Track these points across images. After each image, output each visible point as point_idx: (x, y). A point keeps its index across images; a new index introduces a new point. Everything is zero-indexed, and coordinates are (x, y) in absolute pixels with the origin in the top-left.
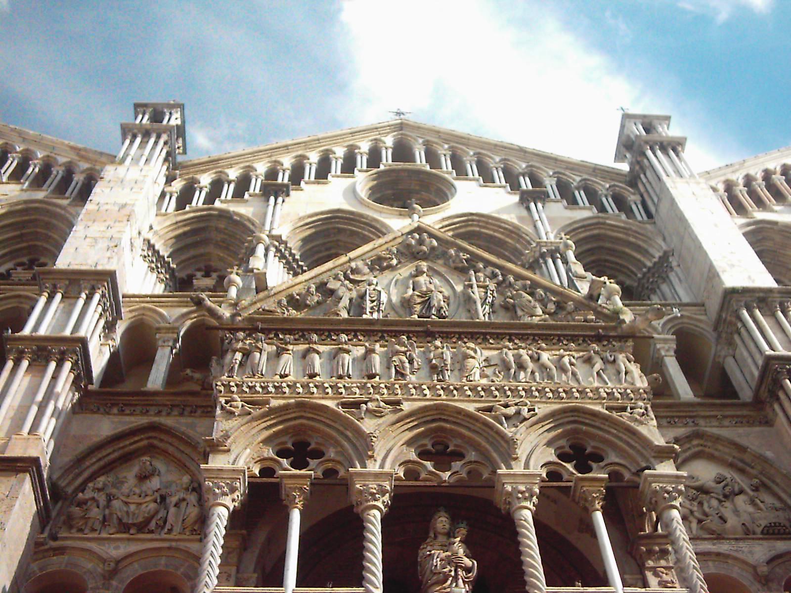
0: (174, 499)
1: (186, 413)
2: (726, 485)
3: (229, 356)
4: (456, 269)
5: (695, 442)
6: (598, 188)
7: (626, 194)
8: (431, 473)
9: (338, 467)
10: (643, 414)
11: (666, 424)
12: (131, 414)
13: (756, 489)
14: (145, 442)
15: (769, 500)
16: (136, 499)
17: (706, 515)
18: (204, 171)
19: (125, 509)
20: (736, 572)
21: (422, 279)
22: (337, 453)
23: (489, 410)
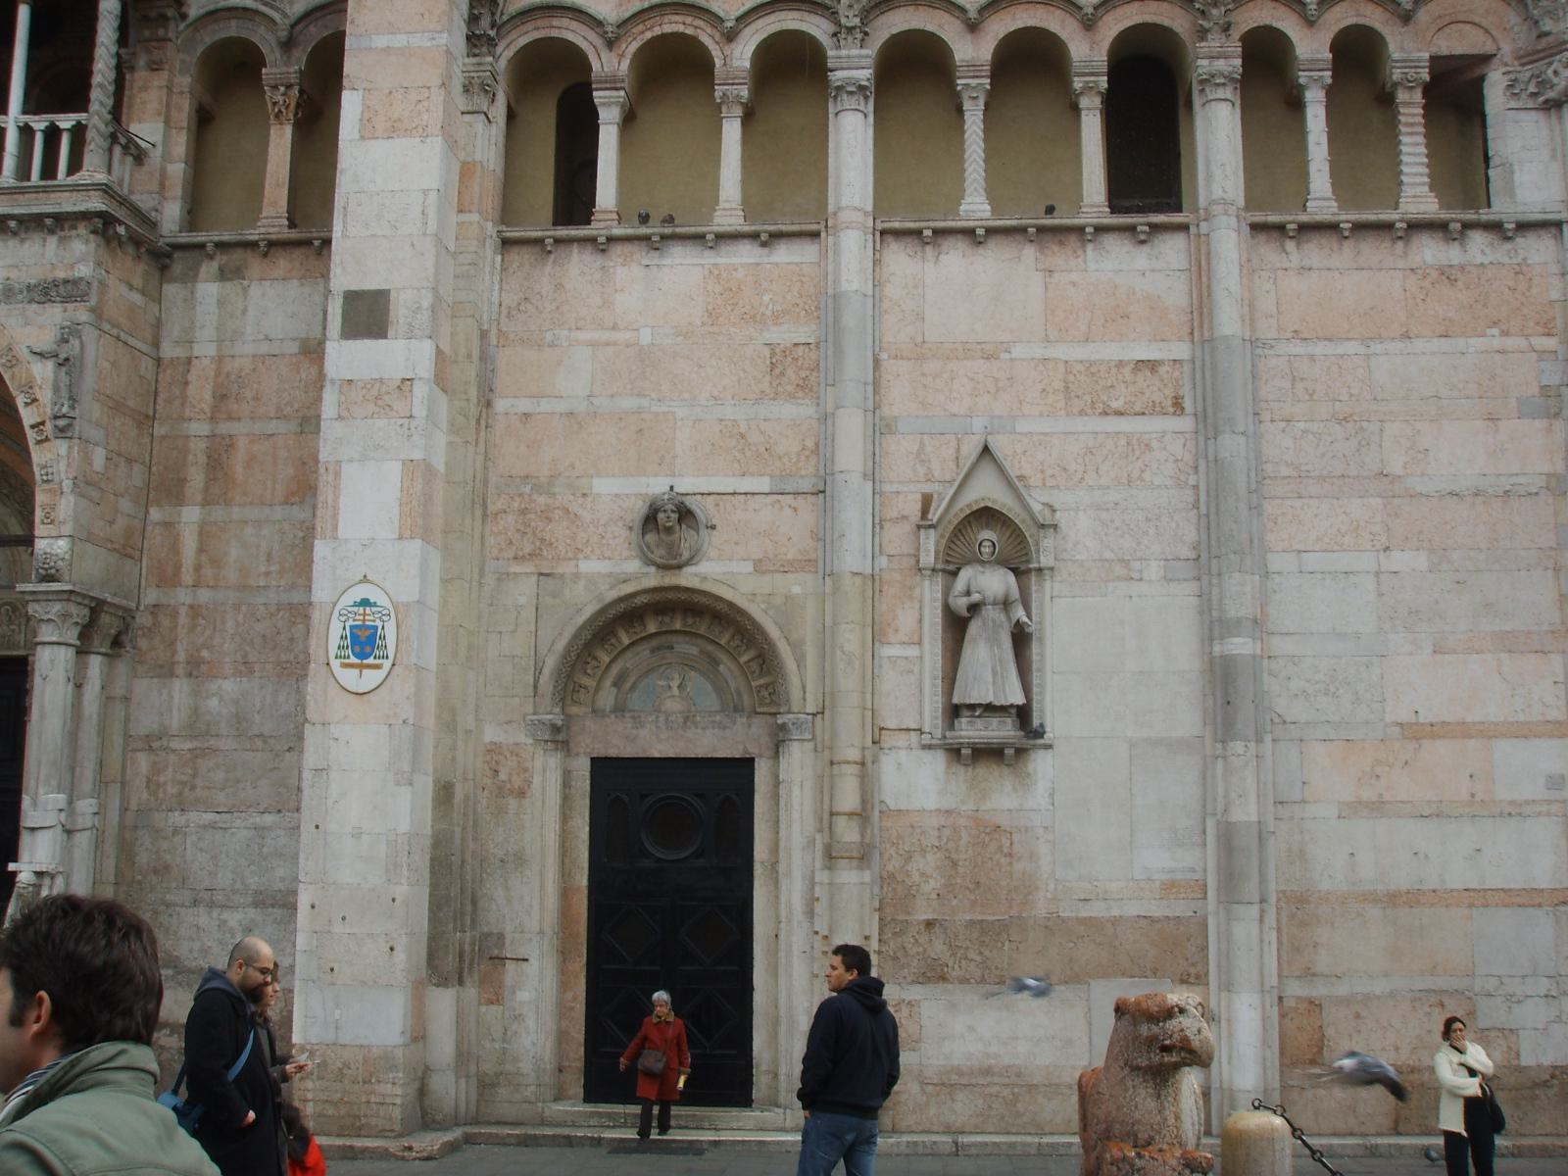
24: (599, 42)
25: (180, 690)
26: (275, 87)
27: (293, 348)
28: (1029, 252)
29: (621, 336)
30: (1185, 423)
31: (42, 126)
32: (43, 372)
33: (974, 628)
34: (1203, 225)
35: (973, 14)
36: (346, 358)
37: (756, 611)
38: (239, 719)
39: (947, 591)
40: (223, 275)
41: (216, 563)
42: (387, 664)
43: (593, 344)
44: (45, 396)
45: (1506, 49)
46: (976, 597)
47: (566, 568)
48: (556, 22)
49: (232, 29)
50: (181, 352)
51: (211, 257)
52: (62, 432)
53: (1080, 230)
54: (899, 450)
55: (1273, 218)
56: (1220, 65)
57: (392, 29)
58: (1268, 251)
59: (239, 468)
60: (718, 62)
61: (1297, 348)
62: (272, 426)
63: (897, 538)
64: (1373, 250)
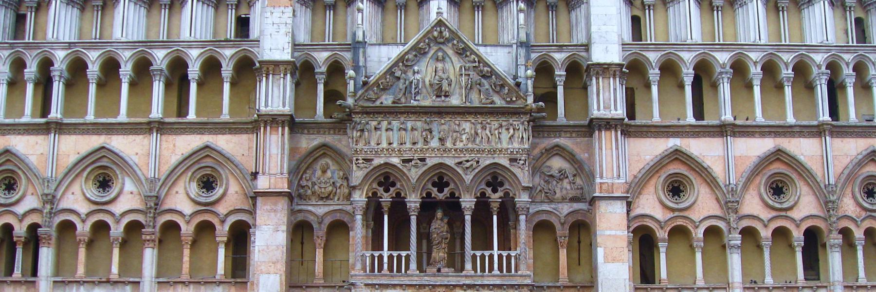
0: (338, 185)
1: (336, 132)
2: (562, 174)
3: (355, 132)
4: (457, 53)
5: (555, 149)
8: (436, 195)
9: (401, 192)
10: (523, 164)
11: (546, 135)
12: (313, 134)
13: (574, 176)
14: (322, 152)
16: (323, 185)
17: (549, 190)
19: (320, 191)
20: (553, 220)
21: (440, 65)
22: (401, 185)
23: (460, 163)
24: (658, 227)
26: (561, 237)
31: (506, 254)
35: (766, 223)
48: (645, 220)
49: (544, 217)
51: (545, 290)
53: (798, 287)
57: (611, 229)
60: (694, 235)
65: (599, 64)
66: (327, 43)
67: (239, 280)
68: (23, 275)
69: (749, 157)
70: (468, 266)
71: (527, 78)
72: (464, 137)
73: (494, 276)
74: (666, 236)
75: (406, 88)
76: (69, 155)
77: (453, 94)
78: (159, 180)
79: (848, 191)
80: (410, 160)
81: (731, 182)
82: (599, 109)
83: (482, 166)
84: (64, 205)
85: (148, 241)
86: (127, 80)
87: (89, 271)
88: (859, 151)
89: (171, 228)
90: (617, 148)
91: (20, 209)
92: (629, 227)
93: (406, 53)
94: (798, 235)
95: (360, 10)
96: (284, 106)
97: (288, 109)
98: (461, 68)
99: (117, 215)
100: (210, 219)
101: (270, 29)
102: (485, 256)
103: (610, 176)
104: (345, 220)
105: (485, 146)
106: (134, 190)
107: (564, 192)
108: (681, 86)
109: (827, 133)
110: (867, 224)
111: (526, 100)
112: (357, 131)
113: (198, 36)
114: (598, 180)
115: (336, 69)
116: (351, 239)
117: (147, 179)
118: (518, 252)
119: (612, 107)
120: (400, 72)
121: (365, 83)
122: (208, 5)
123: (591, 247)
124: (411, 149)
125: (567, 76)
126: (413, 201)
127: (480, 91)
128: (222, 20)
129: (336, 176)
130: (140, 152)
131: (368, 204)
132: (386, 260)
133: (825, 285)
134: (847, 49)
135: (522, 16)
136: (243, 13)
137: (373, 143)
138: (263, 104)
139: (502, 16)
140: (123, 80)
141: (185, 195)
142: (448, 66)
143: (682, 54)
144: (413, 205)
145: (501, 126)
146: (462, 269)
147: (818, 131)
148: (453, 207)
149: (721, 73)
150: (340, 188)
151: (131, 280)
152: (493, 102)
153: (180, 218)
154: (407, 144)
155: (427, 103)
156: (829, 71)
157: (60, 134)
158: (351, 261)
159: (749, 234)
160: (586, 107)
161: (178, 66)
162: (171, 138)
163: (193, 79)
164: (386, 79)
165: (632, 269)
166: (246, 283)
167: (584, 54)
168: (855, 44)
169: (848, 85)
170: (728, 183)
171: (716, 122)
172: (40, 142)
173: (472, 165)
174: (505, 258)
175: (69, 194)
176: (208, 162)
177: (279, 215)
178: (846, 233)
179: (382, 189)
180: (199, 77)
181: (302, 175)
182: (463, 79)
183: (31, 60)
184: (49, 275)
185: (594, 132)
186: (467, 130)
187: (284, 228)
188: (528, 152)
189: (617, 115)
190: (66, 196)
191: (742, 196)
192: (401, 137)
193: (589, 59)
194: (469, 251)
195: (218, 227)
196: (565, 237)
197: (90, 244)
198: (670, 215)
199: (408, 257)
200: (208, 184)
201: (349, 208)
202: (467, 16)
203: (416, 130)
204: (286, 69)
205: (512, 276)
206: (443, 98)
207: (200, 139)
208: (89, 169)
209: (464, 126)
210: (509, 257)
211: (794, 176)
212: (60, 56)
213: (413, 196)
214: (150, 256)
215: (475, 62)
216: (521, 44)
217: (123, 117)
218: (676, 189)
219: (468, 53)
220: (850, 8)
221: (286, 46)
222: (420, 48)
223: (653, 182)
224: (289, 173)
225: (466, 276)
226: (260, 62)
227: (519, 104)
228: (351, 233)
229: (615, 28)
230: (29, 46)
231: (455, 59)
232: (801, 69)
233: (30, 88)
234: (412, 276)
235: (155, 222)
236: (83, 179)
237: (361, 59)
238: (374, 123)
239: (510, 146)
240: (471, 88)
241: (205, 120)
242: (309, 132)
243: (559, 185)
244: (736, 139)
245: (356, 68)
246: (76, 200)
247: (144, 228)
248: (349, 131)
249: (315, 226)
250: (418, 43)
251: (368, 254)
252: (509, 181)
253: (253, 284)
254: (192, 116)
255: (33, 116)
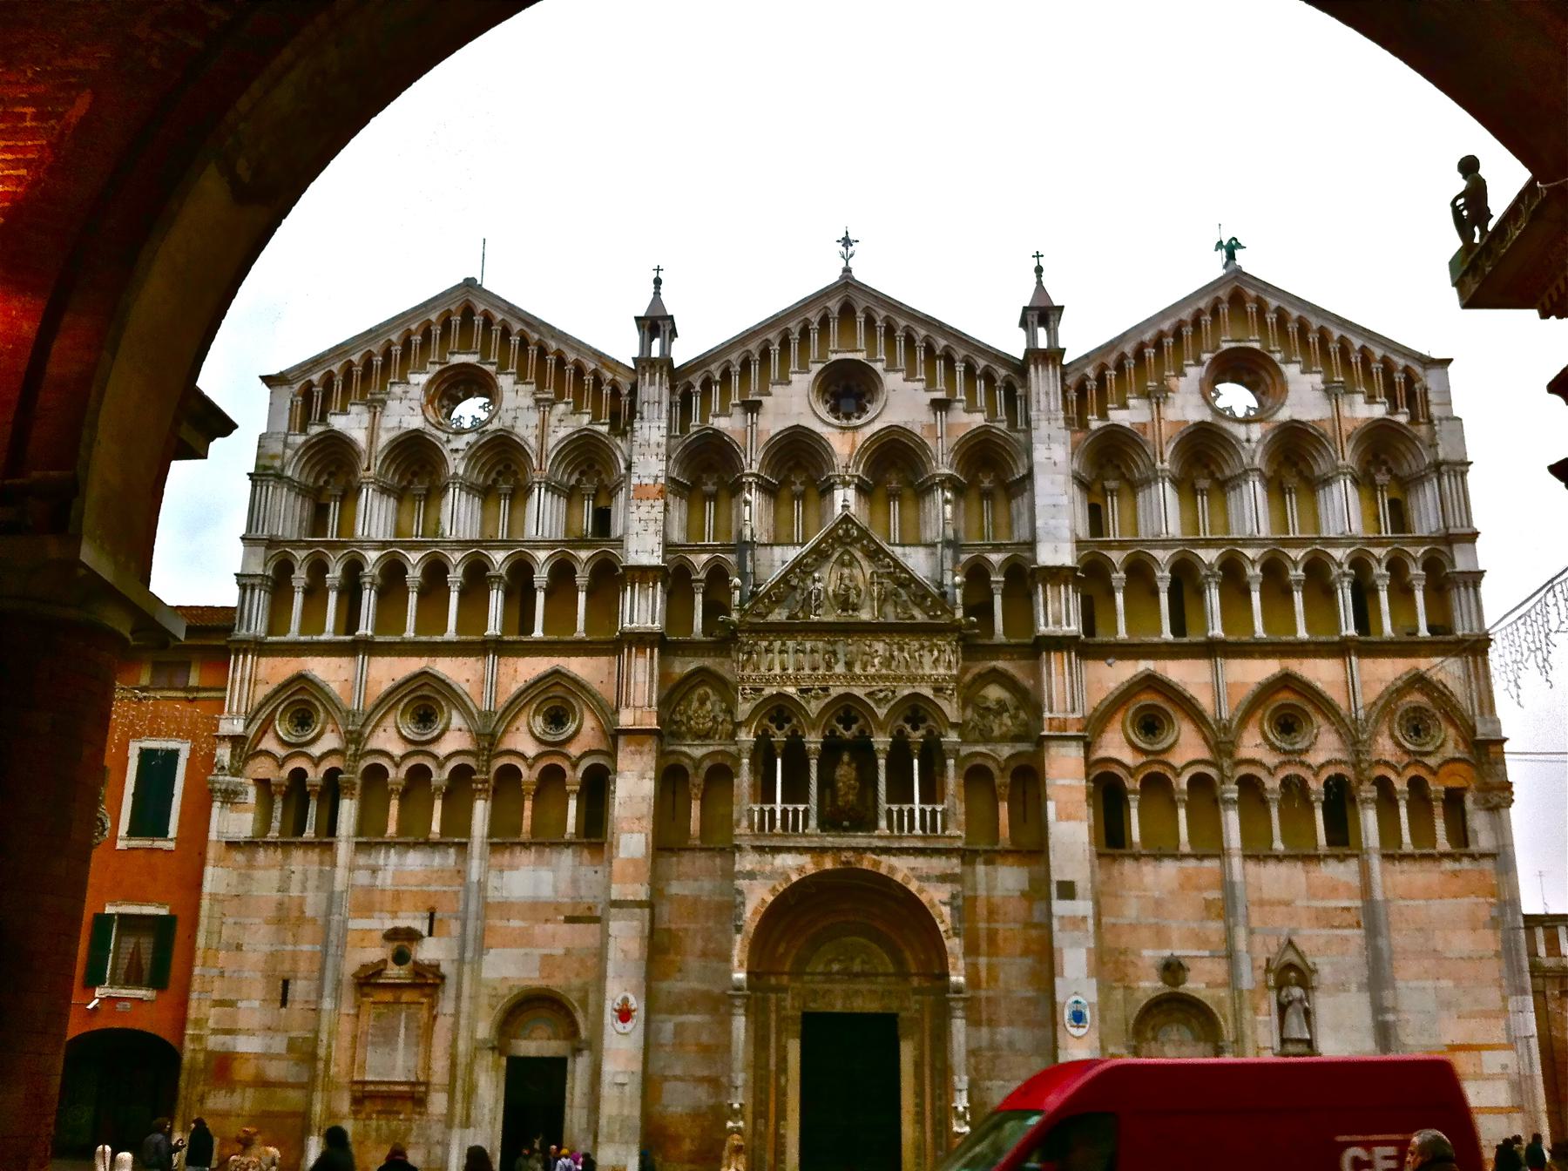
0: (720, 720)
6: (996, 376)
7: (1017, 386)
10: (950, 695)
15: (1022, 715)
18: (695, 371)
20: (991, 764)
21: (846, 571)
23: (870, 694)
25: (985, 1031)
27: (1018, 894)
28: (1300, 865)
29: (1148, 894)
30: (1361, 932)
32: (946, 910)
33: (1290, 1010)
34: (1365, 856)
36: (1060, 907)
37: (1208, 1003)
38: (1011, 1044)
39: (1279, 995)
40: (989, 862)
41: (996, 980)
42: (1088, 1026)
43: (1137, 897)
44: (948, 920)
45: (1473, 786)
46: (1290, 998)
47: (1134, 985)
49: (978, 761)
50: (970, 893)
52: (956, 935)
54: (1258, 939)
55: (1390, 852)
56: (1369, 795)
57: (1064, 777)
58: (1389, 866)
59: (1001, 943)
60: (1174, 785)
61: (1401, 902)
62: (1012, 925)
63: (1260, 975)
64: (1428, 865)
65: (1046, 568)
66: (706, 543)
67: (593, 840)
68: (317, 835)
69: (1244, 684)
70: (883, 824)
71: (955, 586)
72: (876, 661)
73: (916, 837)
74: (1138, 787)
75: (804, 599)
76: (381, 682)
77: (862, 608)
78: (496, 713)
79: (1385, 729)
80: (810, 690)
81: (1223, 716)
82: (1046, 624)
83: (899, 697)
84: (374, 744)
85: (480, 790)
86: (456, 588)
87: (401, 830)
88: (1398, 675)
89: (510, 773)
90: (1071, 674)
91: (316, 750)
92: (1087, 775)
93: (805, 557)
94: (1316, 786)
95: (747, 503)
96: (653, 622)
97: (657, 626)
98: (872, 574)
99: (441, 758)
100: (559, 763)
101: (636, 527)
102: (903, 811)
103: (1062, 708)
104: (729, 763)
105: (903, 671)
106: (465, 727)
107: (1004, 729)
108: (1155, 593)
109: (1352, 652)
110: (1411, 772)
111: (954, 615)
112: (743, 654)
113: (547, 534)
114: (1047, 715)
115: (718, 574)
116: (735, 789)
117: (480, 712)
118: (945, 806)
119: (1064, 622)
120: (796, 581)
121: (754, 594)
122: (559, 496)
123: (1040, 799)
124: (810, 676)
125: (1005, 583)
126: (813, 740)
127: (896, 602)
128: (576, 511)
129: (717, 708)
130: (472, 679)
131: (756, 744)
132: (778, 815)
133: (1355, 852)
134: (1378, 542)
135: (948, 508)
136: (602, 503)
137: (762, 669)
138: (627, 619)
139: (924, 507)
140: (452, 588)
141: (529, 735)
142: (857, 572)
143: (1154, 553)
144: (813, 746)
145: (922, 647)
146: (876, 827)
147: (1341, 650)
148: (863, 751)
149: (1207, 576)
150: (722, 723)
151: (456, 840)
152: (913, 617)
153: (521, 761)
154: (806, 669)
155: (831, 618)
156: (1353, 572)
157: (371, 655)
158: (735, 816)
159: (1250, 786)
160: (1031, 621)
161: (521, 570)
162: (511, 660)
163: (540, 587)
164: (779, 588)
165: (1094, 830)
166: (603, 844)
167: (1027, 555)
168: (1390, 535)
169: (1380, 588)
170: (1218, 717)
171: (1202, 639)
172: (343, 665)
173: (886, 696)
174: (928, 813)
175: (380, 731)
176: (559, 691)
177: (645, 758)
178: (1383, 784)
179: (773, 726)
180: (547, 584)
181: (675, 708)
182: (875, 588)
183: (334, 561)
184: (352, 834)
185: (1041, 654)
186: (880, 653)
187: (652, 774)
188: (957, 679)
189: (1072, 631)
190: (375, 734)
191: (1239, 735)
192: (797, 661)
193: (1034, 561)
194: (883, 805)
195: (569, 772)
196: (1006, 787)
197: (404, 796)
198: (1143, 759)
199: (806, 812)
200: (557, 718)
201: (733, 749)
202: (880, 509)
203: (817, 652)
204: (655, 576)
205: (939, 837)
206: (850, 612)
207: (549, 661)
208: (406, 700)
209: (877, 648)
210: (934, 812)
211: (1309, 708)
212: (372, 556)
213: (813, 734)
214: (481, 810)
215: (890, 567)
216: (948, 544)
217: (451, 634)
218: (1150, 724)
219: (881, 556)
220: (1382, 486)
221: (656, 548)
222: (822, 551)
223: (1119, 717)
224: (659, 704)
225: (880, 837)
226: (623, 567)
227: (945, 620)
228: (735, 780)
229: (1067, 522)
230: (332, 546)
231: (865, 563)
232: (1317, 568)
233: (333, 597)
234: (811, 836)
235: (488, 767)
236: (399, 712)
237: (749, 563)
238: (765, 644)
239: (934, 672)
240: (885, 600)
241: (555, 637)
242: (683, 653)
243: (997, 721)
244: (1229, 661)
245: (743, 575)
246: (389, 739)
247: (475, 774)
248: (733, 654)
249: (691, 771)
250: (819, 543)
251: (756, 808)
252: (934, 718)
253: (611, 845)
254: (538, 633)
255: (336, 632)
